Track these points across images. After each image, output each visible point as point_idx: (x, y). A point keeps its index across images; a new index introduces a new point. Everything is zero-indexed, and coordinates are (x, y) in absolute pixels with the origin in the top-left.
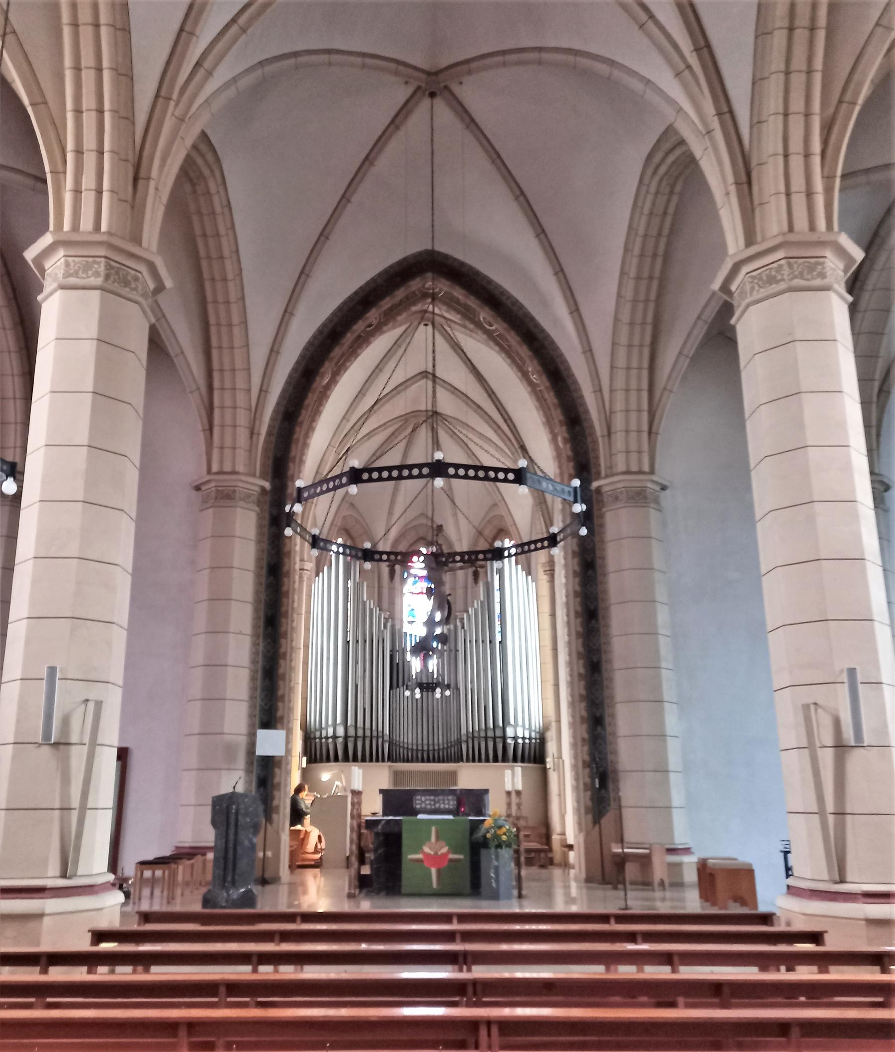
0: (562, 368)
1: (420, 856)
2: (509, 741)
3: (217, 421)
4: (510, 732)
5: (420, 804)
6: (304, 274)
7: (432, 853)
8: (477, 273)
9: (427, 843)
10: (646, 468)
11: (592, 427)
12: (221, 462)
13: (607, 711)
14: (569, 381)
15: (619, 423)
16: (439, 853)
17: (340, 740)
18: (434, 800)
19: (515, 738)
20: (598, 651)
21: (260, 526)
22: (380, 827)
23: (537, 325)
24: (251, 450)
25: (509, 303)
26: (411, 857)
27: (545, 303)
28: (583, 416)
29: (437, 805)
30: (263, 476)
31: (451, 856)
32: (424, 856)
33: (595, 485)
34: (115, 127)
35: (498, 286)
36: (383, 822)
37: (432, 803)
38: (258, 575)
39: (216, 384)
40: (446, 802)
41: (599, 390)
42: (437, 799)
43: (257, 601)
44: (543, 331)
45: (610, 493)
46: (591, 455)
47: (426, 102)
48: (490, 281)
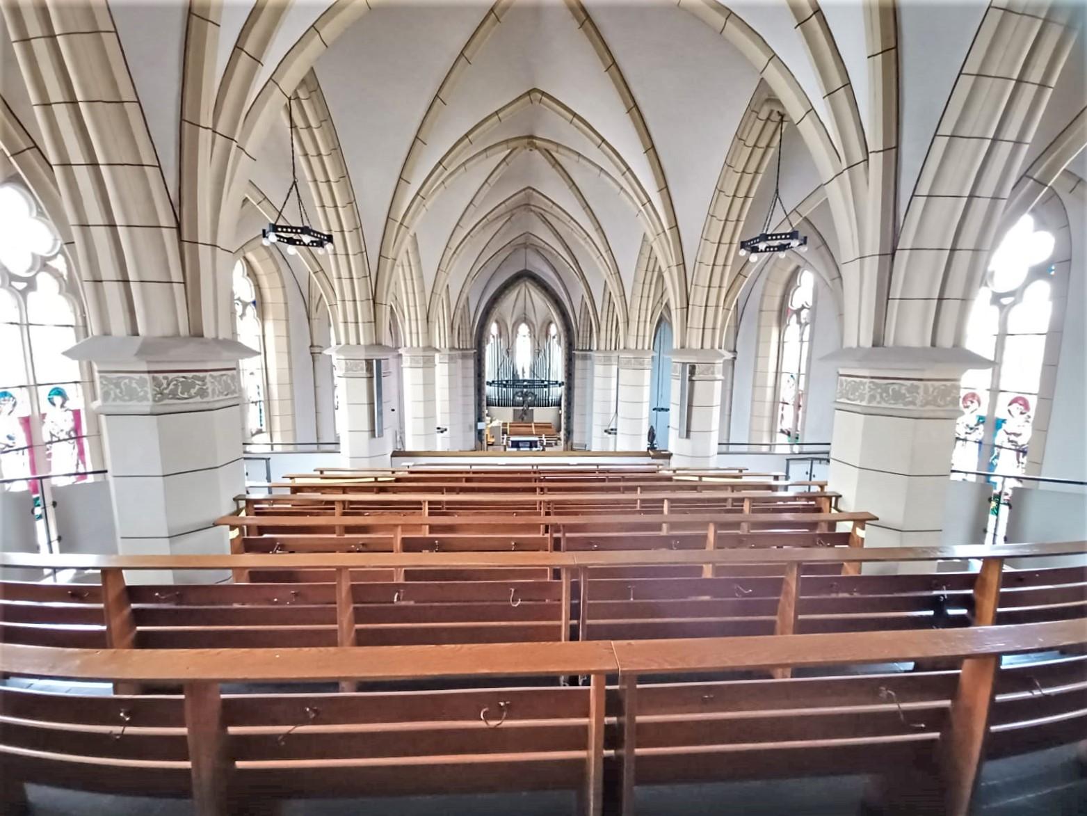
2: (550, 401)
4: (550, 398)
6: (486, 287)
10: (588, 348)
12: (463, 345)
15: (581, 334)
17: (497, 401)
19: (552, 400)
21: (475, 363)
24: (471, 340)
27: (560, 290)
30: (475, 349)
33: (573, 352)
34: (448, 322)
38: (475, 378)
41: (576, 323)
43: (475, 385)
47: (524, 250)
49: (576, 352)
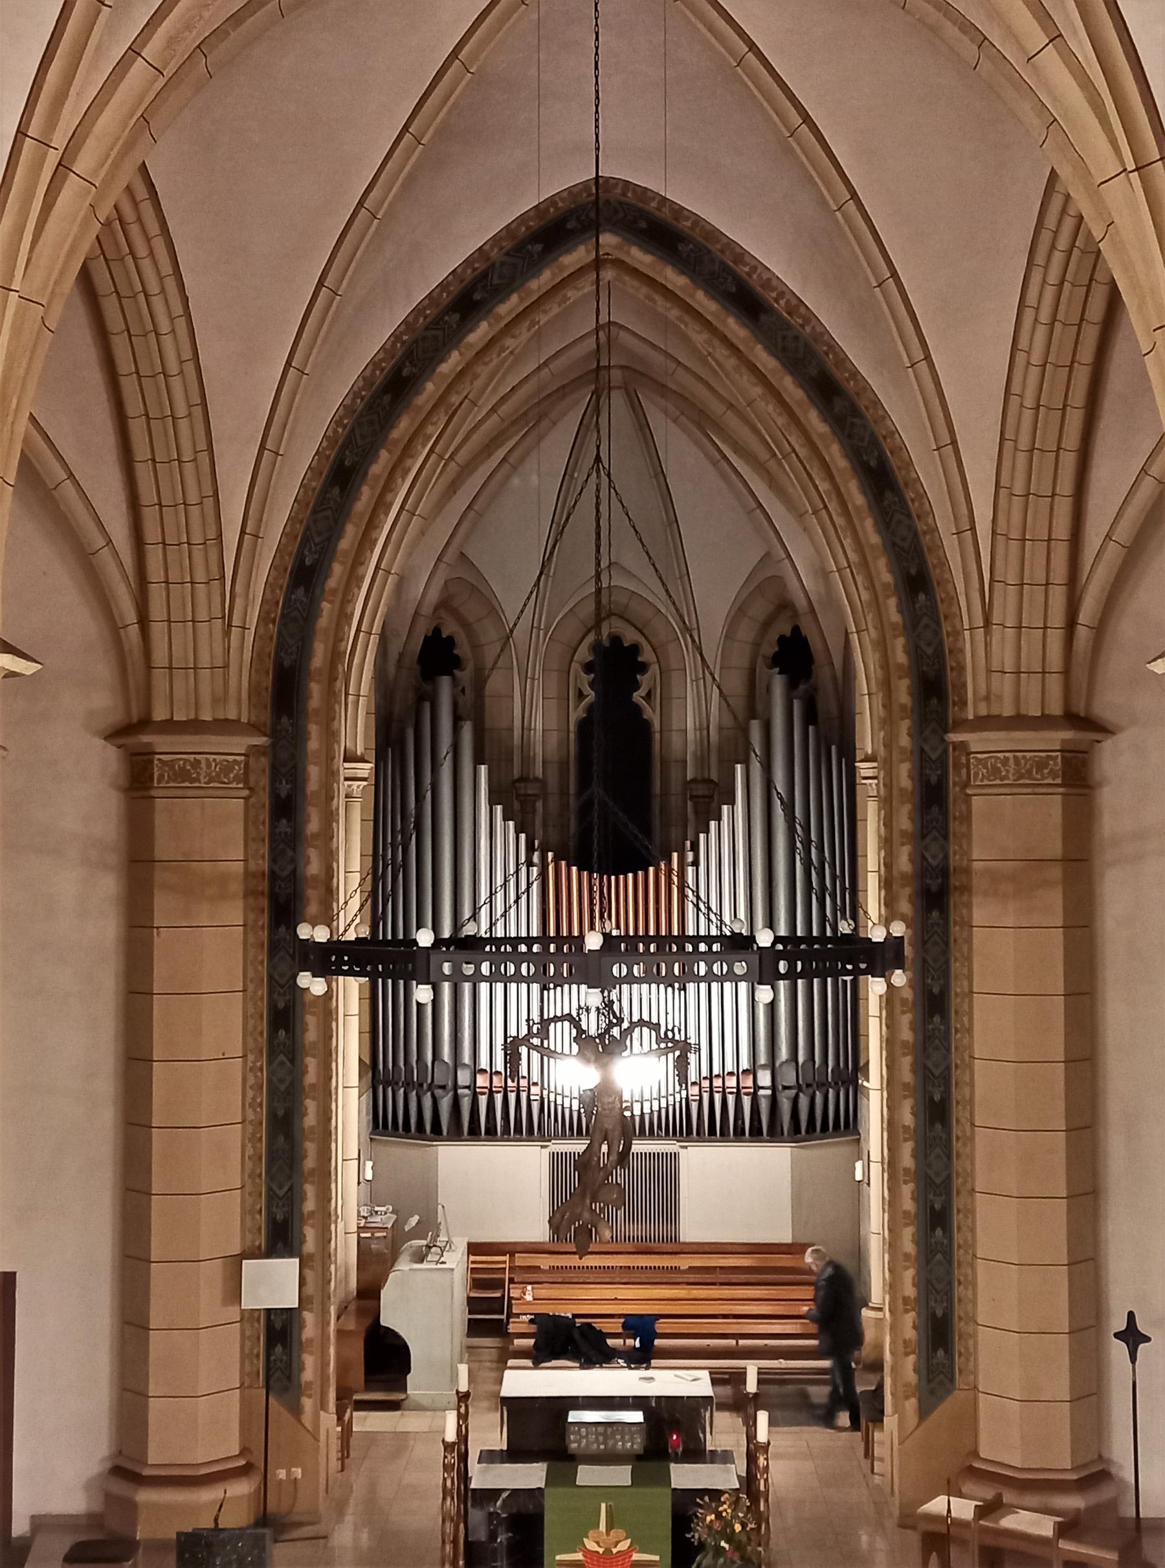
0: (894, 462)
1: (579, 1556)
3: (157, 610)
5: (579, 1443)
7: (601, 1550)
8: (714, 234)
9: (591, 1533)
11: (953, 599)
13: (958, 1202)
14: (909, 495)
15: (1004, 611)
16: (615, 1551)
18: (605, 1434)
20: (945, 1079)
22: (499, 1503)
23: (842, 360)
25: (780, 306)
26: (558, 1557)
28: (935, 574)
29: (611, 1443)
31: (636, 1557)
32: (584, 1556)
35: (757, 266)
36: (505, 1495)
37: (601, 1438)
39: (152, 533)
40: (627, 1437)
42: (609, 1430)
44: (855, 374)
45: (979, 756)
46: (950, 662)
48: (741, 255)
49: (976, 741)
